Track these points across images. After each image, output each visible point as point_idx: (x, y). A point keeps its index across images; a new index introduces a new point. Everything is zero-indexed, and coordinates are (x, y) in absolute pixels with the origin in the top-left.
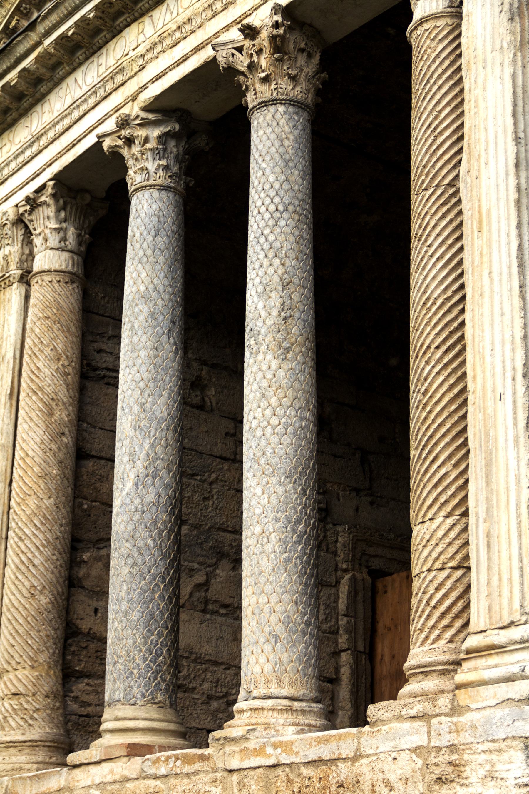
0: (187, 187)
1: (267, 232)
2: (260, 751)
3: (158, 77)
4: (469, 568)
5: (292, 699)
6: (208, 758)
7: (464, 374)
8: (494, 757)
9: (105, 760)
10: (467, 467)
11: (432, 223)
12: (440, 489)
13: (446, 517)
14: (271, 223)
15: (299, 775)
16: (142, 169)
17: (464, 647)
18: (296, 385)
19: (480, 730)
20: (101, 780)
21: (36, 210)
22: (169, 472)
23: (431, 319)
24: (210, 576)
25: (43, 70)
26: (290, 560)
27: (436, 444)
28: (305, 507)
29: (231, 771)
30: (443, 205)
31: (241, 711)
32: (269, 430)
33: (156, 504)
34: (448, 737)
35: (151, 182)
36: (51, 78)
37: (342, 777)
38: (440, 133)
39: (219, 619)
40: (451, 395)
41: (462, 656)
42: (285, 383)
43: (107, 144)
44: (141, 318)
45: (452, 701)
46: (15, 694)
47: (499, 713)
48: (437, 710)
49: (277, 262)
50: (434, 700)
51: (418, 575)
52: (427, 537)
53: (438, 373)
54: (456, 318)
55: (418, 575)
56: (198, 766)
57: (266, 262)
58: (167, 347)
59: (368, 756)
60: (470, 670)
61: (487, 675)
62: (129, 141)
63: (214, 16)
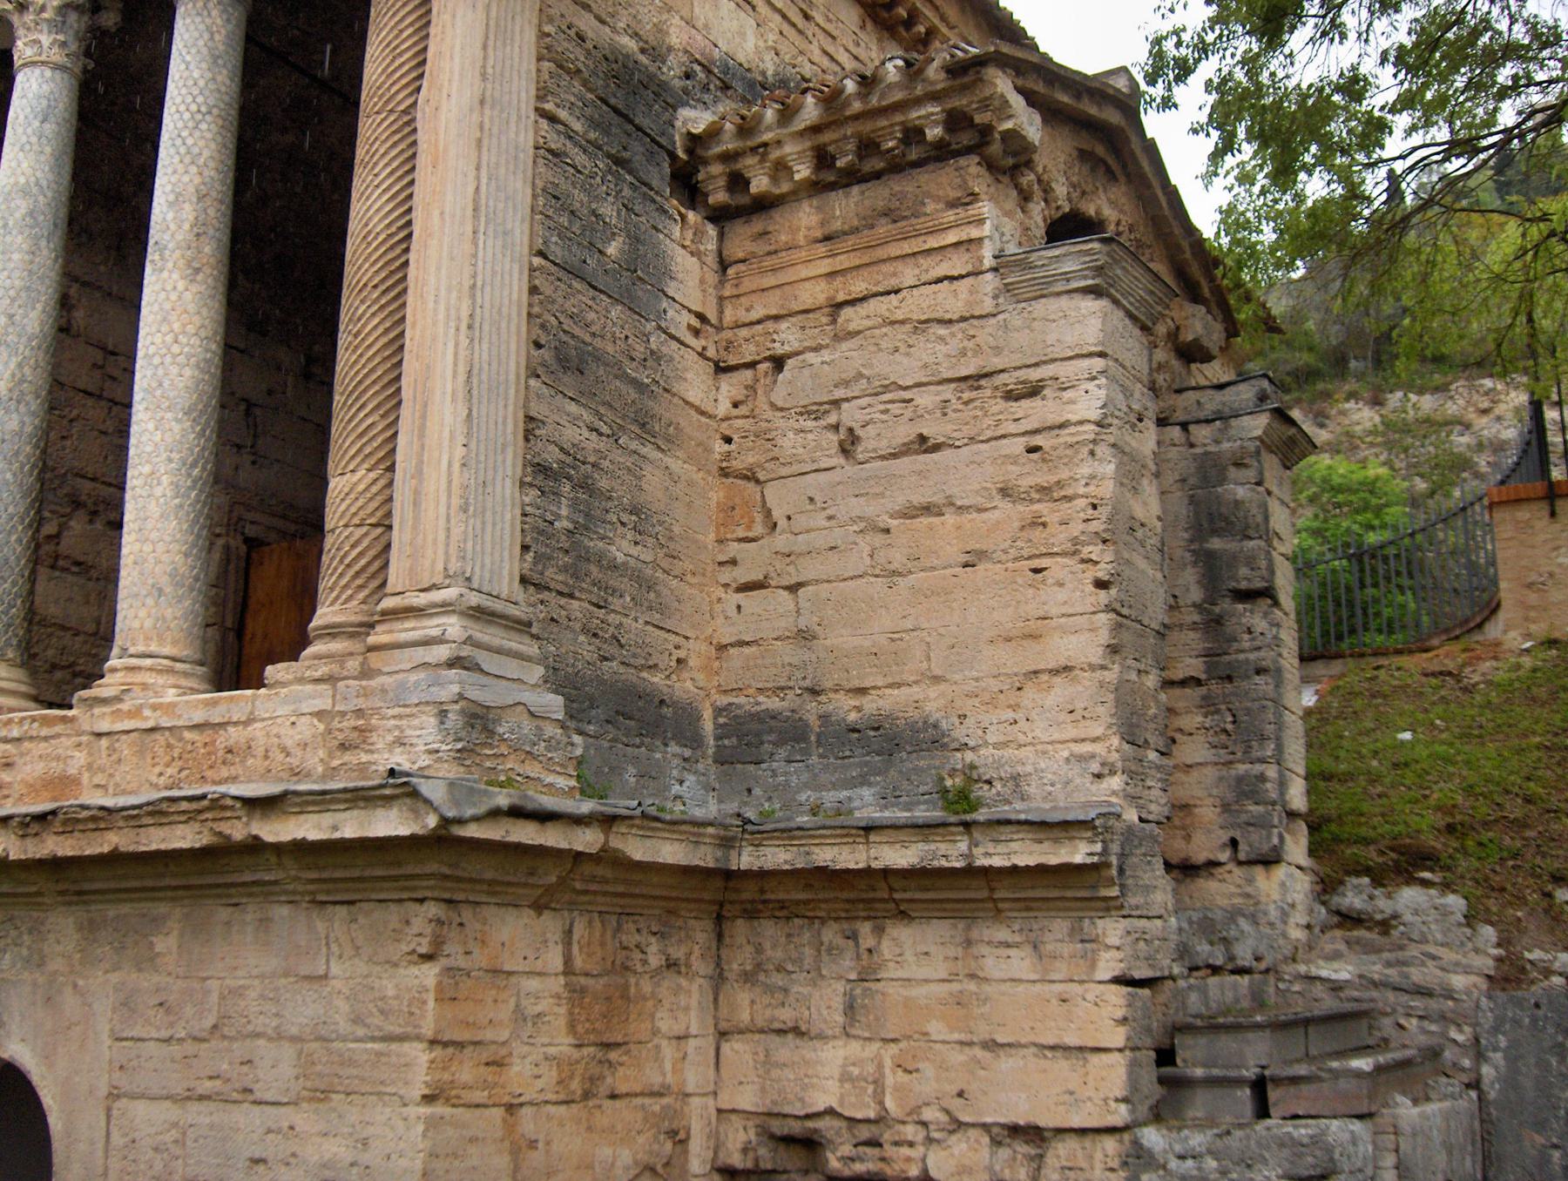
0: (85, 71)
1: (185, 134)
2: (136, 713)
4: (390, 527)
5: (174, 659)
6: (72, 720)
7: (404, 318)
8: (404, 722)
10: (398, 418)
11: (382, 151)
12: (365, 440)
13: (369, 470)
14: (191, 124)
15: (181, 739)
17: (379, 608)
18: (205, 312)
19: (391, 694)
22: (38, 397)
23: (370, 255)
24: (62, 528)
26: (181, 506)
27: (365, 391)
28: (203, 449)
29: (99, 735)
30: (395, 132)
31: (114, 670)
32: (168, 359)
33: (19, 434)
34: (355, 701)
35: (43, 58)
37: (231, 742)
38: (400, 55)
39: (70, 578)
40: (385, 340)
41: (376, 618)
42: (192, 308)
44: (18, 215)
45: (362, 664)
47: (413, 677)
48: (345, 673)
49: (194, 169)
50: (342, 665)
51: (333, 531)
52: (346, 490)
53: (374, 315)
54: (399, 257)
55: (333, 531)
56: (58, 729)
57: (181, 168)
58: (45, 252)
59: (263, 720)
60: (384, 632)
61: (403, 637)
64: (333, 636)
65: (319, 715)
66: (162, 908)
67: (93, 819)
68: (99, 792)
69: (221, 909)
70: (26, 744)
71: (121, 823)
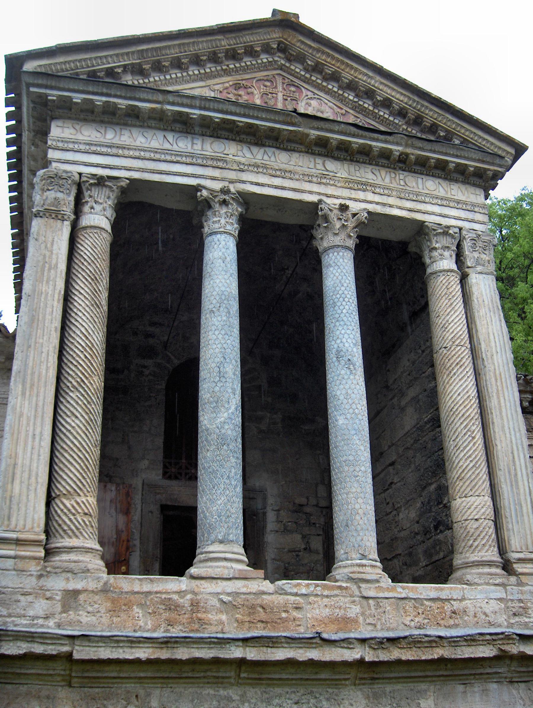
3: (257, 184)
9: (236, 578)
15: (422, 605)
16: (232, 224)
20: (234, 591)
21: (100, 187)
25: (146, 116)
34: (517, 595)
36: (144, 122)
43: (205, 193)
46: (86, 514)
59: (470, 599)
62: (224, 203)
63: (310, 182)
64: (490, 566)
65: (500, 600)
66: (423, 686)
67: (430, 642)
68: (370, 628)
69: (458, 686)
70: (312, 599)
71: (446, 644)
